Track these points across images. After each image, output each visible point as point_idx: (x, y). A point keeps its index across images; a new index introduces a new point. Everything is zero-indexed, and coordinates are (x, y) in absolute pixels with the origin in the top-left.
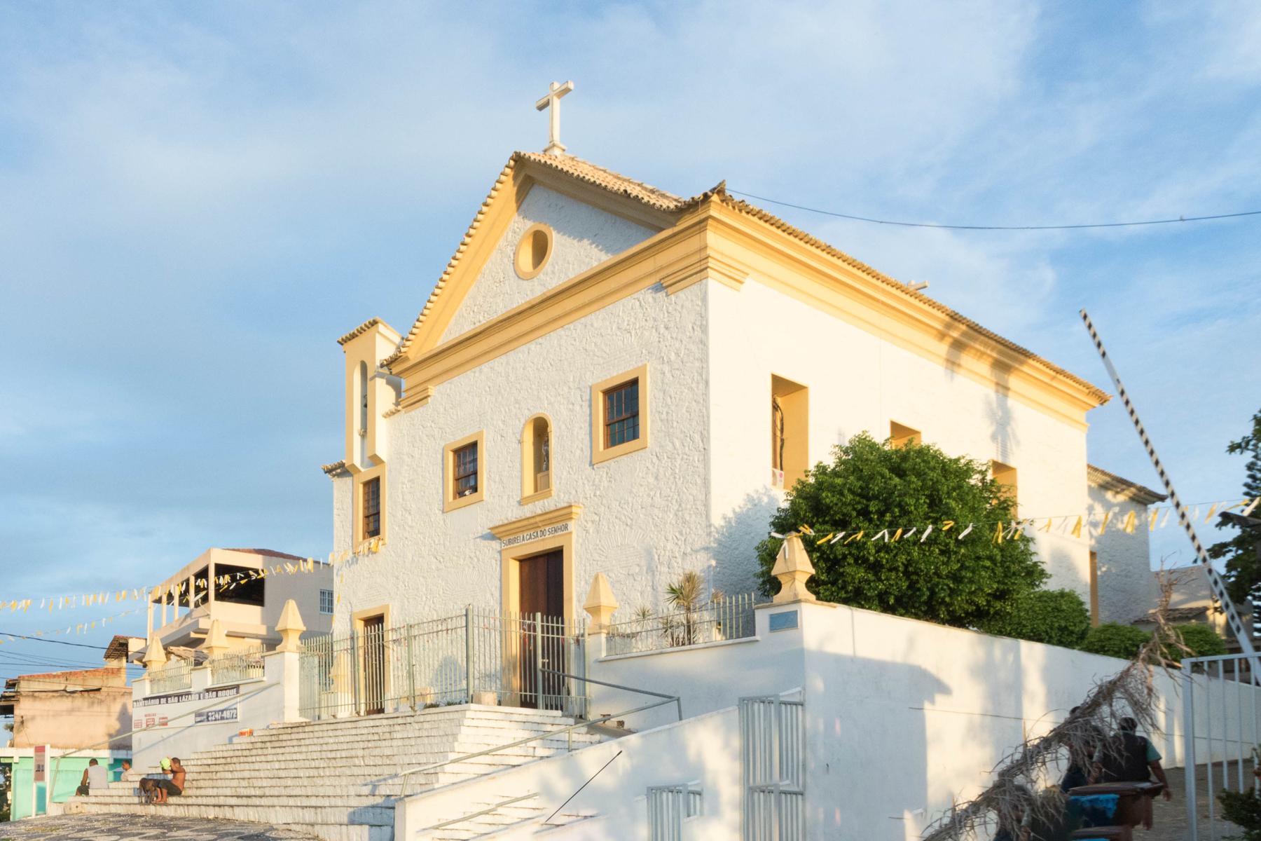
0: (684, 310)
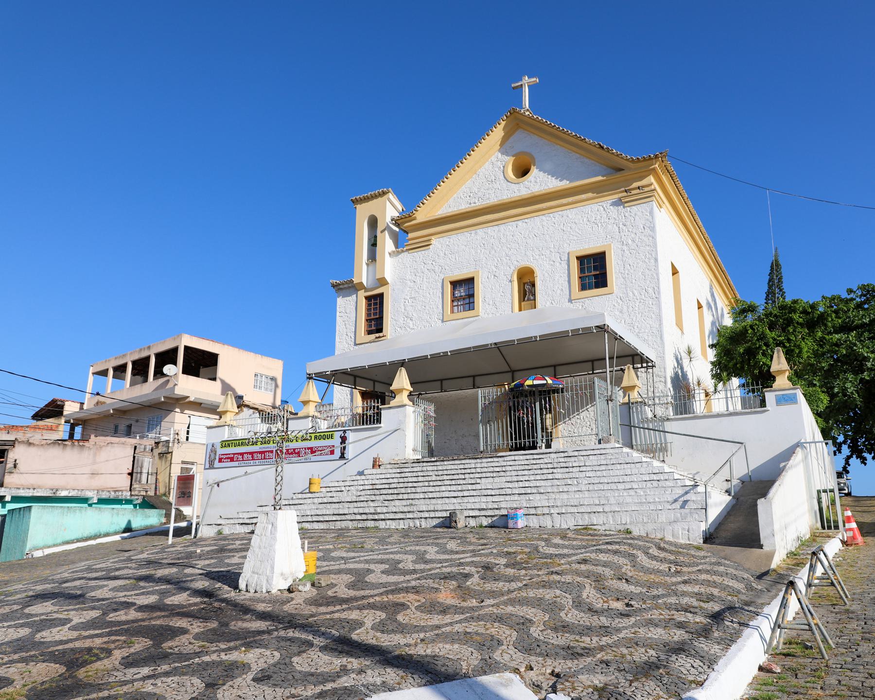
0: (637, 217)
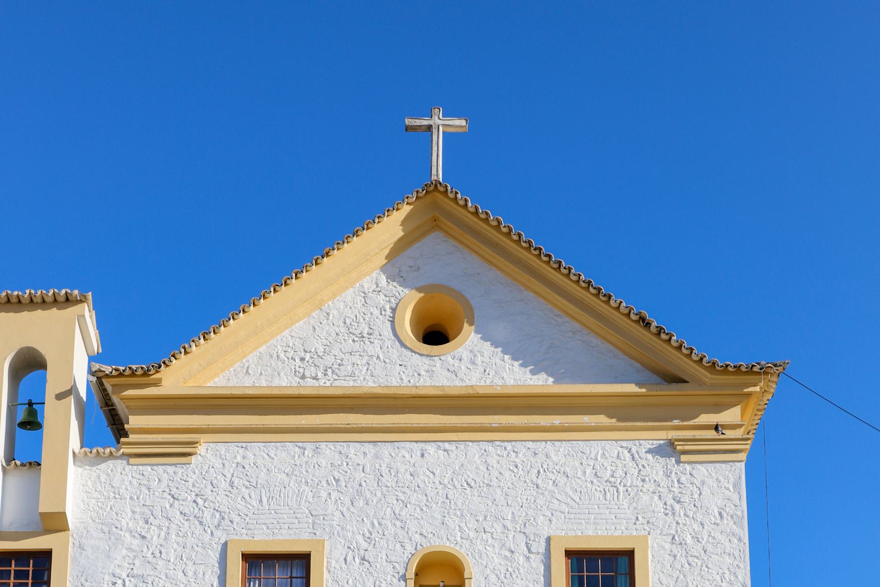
0: (706, 488)
